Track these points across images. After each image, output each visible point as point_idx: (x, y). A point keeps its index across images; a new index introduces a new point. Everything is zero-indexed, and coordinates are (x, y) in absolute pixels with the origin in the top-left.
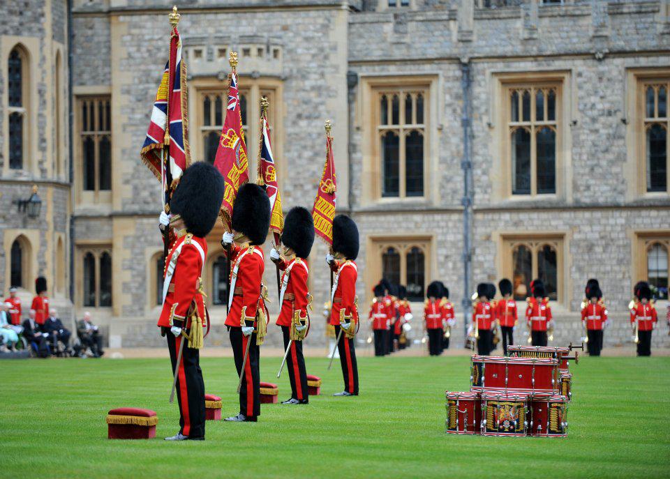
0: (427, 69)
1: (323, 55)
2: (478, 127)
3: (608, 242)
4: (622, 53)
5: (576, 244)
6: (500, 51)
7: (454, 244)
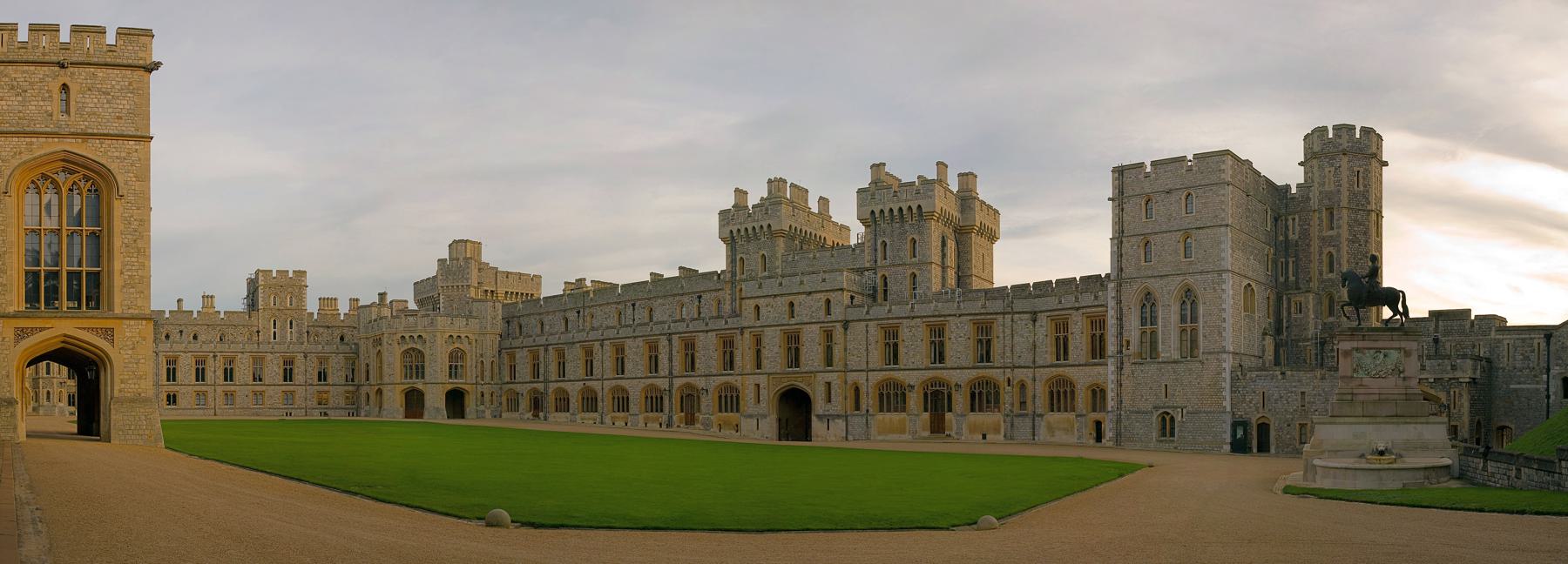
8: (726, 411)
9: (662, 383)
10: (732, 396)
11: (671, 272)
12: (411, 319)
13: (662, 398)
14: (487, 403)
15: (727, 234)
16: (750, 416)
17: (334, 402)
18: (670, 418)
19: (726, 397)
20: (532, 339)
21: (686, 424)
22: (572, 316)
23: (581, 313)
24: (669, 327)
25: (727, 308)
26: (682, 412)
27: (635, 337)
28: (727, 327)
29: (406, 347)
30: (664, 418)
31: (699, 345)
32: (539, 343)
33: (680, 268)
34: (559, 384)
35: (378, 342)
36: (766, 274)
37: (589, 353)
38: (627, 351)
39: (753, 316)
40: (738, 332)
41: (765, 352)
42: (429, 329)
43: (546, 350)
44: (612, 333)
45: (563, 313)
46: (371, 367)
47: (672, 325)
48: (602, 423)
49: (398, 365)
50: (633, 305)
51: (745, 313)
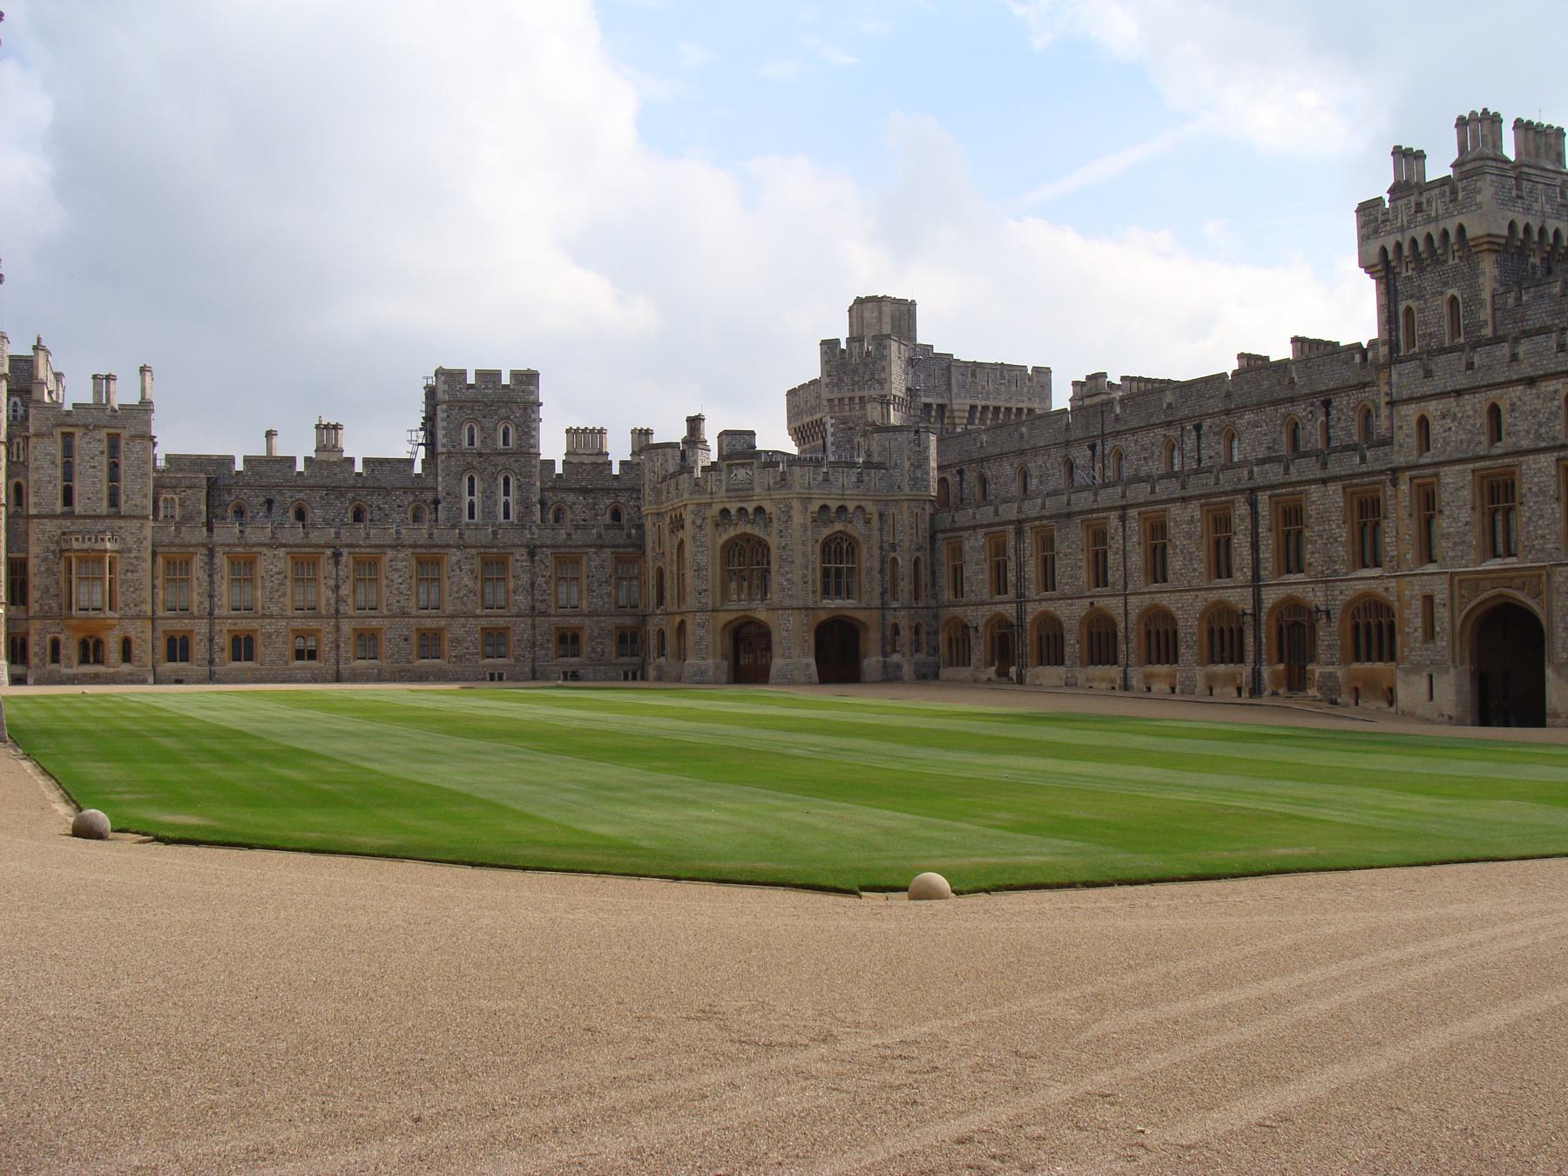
0: (191, 549)
1: (140, 541)
2: (216, 578)
3: (278, 633)
4: (285, 546)
5: (263, 634)
6: (227, 542)
7: (204, 633)
8: (1369, 660)
9: (1240, 599)
10: (1380, 626)
11: (1281, 351)
12: (741, 473)
13: (1241, 631)
14: (906, 649)
15: (1374, 258)
16: (1416, 669)
17: (594, 650)
18: (1256, 675)
19: (1368, 626)
20: (991, 509)
21: (1290, 688)
22: (1081, 455)
23: (1099, 448)
24: (1251, 472)
25: (1381, 425)
26: (1281, 661)
27: (1184, 499)
28: (1364, 468)
29: (732, 532)
30: (1245, 670)
31: (1311, 511)
32: (1006, 517)
33: (1295, 340)
34: (1045, 606)
35: (678, 524)
36: (1462, 340)
37: (1099, 537)
38: (1172, 530)
39: (1413, 441)
40: (1386, 478)
41: (1442, 524)
42: (777, 495)
43: (1019, 533)
44: (1140, 492)
45: (1063, 451)
46: (667, 576)
47: (1255, 468)
48: (1126, 687)
49: (714, 570)
50: (1198, 428)
51: (1399, 437)
